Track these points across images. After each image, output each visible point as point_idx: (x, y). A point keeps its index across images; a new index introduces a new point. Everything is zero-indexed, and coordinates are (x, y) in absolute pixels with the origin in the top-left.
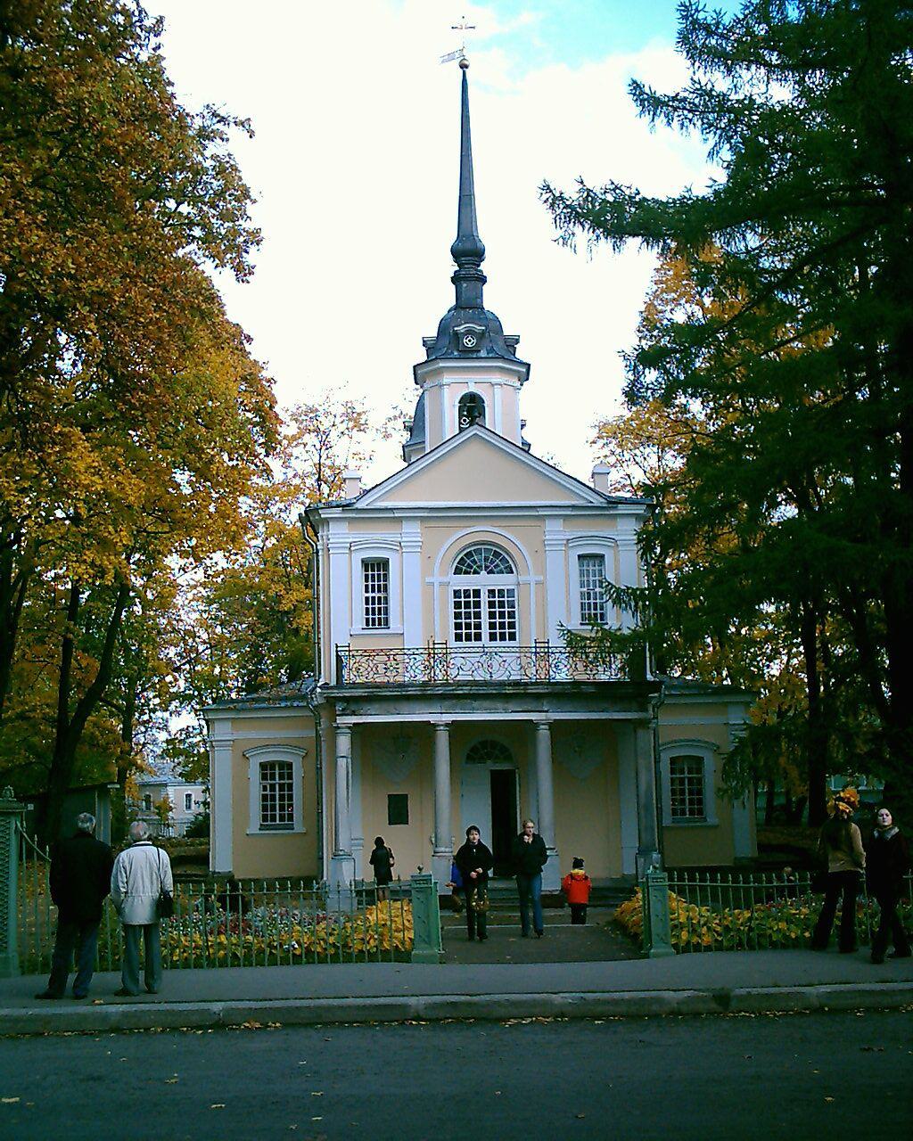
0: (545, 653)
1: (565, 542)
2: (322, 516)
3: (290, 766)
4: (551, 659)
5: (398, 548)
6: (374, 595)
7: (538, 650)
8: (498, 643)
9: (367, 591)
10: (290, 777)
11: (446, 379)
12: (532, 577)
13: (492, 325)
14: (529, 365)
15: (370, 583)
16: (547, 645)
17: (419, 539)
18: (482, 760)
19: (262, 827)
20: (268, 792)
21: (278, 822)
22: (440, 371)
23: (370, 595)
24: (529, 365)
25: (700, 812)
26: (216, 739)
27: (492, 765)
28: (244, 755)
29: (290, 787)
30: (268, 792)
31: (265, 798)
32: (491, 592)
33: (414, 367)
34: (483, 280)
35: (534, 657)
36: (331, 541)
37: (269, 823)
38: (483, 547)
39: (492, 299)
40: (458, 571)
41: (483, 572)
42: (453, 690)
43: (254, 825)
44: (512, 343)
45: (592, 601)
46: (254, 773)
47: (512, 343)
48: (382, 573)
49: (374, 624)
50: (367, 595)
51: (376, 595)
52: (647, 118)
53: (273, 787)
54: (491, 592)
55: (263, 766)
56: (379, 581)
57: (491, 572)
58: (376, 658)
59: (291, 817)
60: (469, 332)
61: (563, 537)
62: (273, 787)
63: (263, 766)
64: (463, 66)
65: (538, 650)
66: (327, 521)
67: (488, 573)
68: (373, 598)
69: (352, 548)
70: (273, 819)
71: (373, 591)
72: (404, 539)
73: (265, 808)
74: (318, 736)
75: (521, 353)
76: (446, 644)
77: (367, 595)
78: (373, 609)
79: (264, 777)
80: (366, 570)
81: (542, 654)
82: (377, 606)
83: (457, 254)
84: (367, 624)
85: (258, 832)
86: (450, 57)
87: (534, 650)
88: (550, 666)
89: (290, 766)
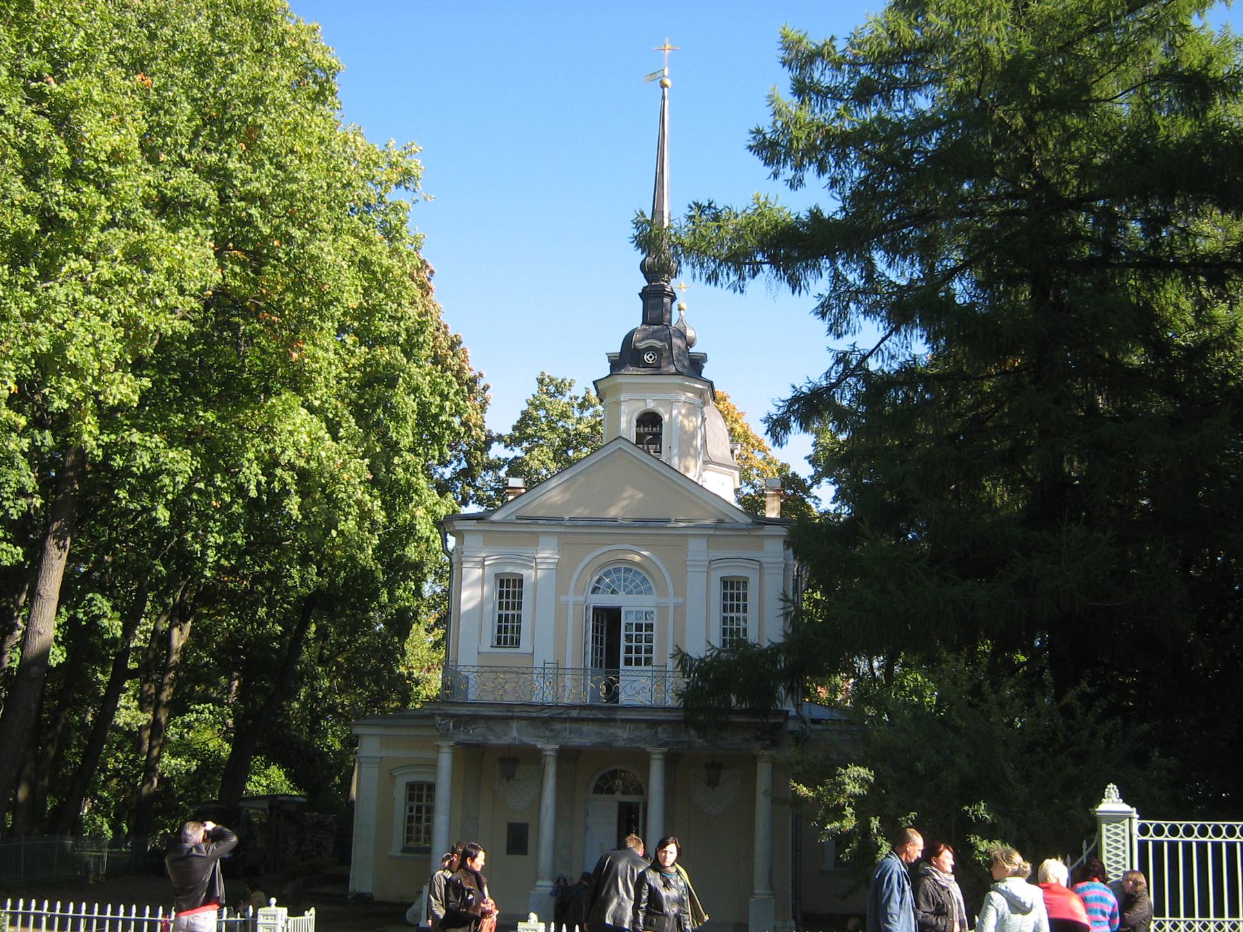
8: (633, 667)
9: (501, 608)
12: (671, 600)
16: (664, 669)
18: (611, 791)
19: (405, 850)
23: (504, 612)
26: (365, 755)
27: (619, 797)
30: (414, 813)
31: (410, 819)
35: (649, 682)
40: (595, 590)
43: (396, 850)
46: (400, 793)
48: (517, 590)
49: (505, 643)
51: (510, 612)
53: (419, 809)
56: (514, 598)
57: (630, 593)
58: (485, 675)
71: (507, 608)
73: (409, 830)
79: (411, 798)
80: (501, 586)
84: (499, 643)
85: (399, 854)
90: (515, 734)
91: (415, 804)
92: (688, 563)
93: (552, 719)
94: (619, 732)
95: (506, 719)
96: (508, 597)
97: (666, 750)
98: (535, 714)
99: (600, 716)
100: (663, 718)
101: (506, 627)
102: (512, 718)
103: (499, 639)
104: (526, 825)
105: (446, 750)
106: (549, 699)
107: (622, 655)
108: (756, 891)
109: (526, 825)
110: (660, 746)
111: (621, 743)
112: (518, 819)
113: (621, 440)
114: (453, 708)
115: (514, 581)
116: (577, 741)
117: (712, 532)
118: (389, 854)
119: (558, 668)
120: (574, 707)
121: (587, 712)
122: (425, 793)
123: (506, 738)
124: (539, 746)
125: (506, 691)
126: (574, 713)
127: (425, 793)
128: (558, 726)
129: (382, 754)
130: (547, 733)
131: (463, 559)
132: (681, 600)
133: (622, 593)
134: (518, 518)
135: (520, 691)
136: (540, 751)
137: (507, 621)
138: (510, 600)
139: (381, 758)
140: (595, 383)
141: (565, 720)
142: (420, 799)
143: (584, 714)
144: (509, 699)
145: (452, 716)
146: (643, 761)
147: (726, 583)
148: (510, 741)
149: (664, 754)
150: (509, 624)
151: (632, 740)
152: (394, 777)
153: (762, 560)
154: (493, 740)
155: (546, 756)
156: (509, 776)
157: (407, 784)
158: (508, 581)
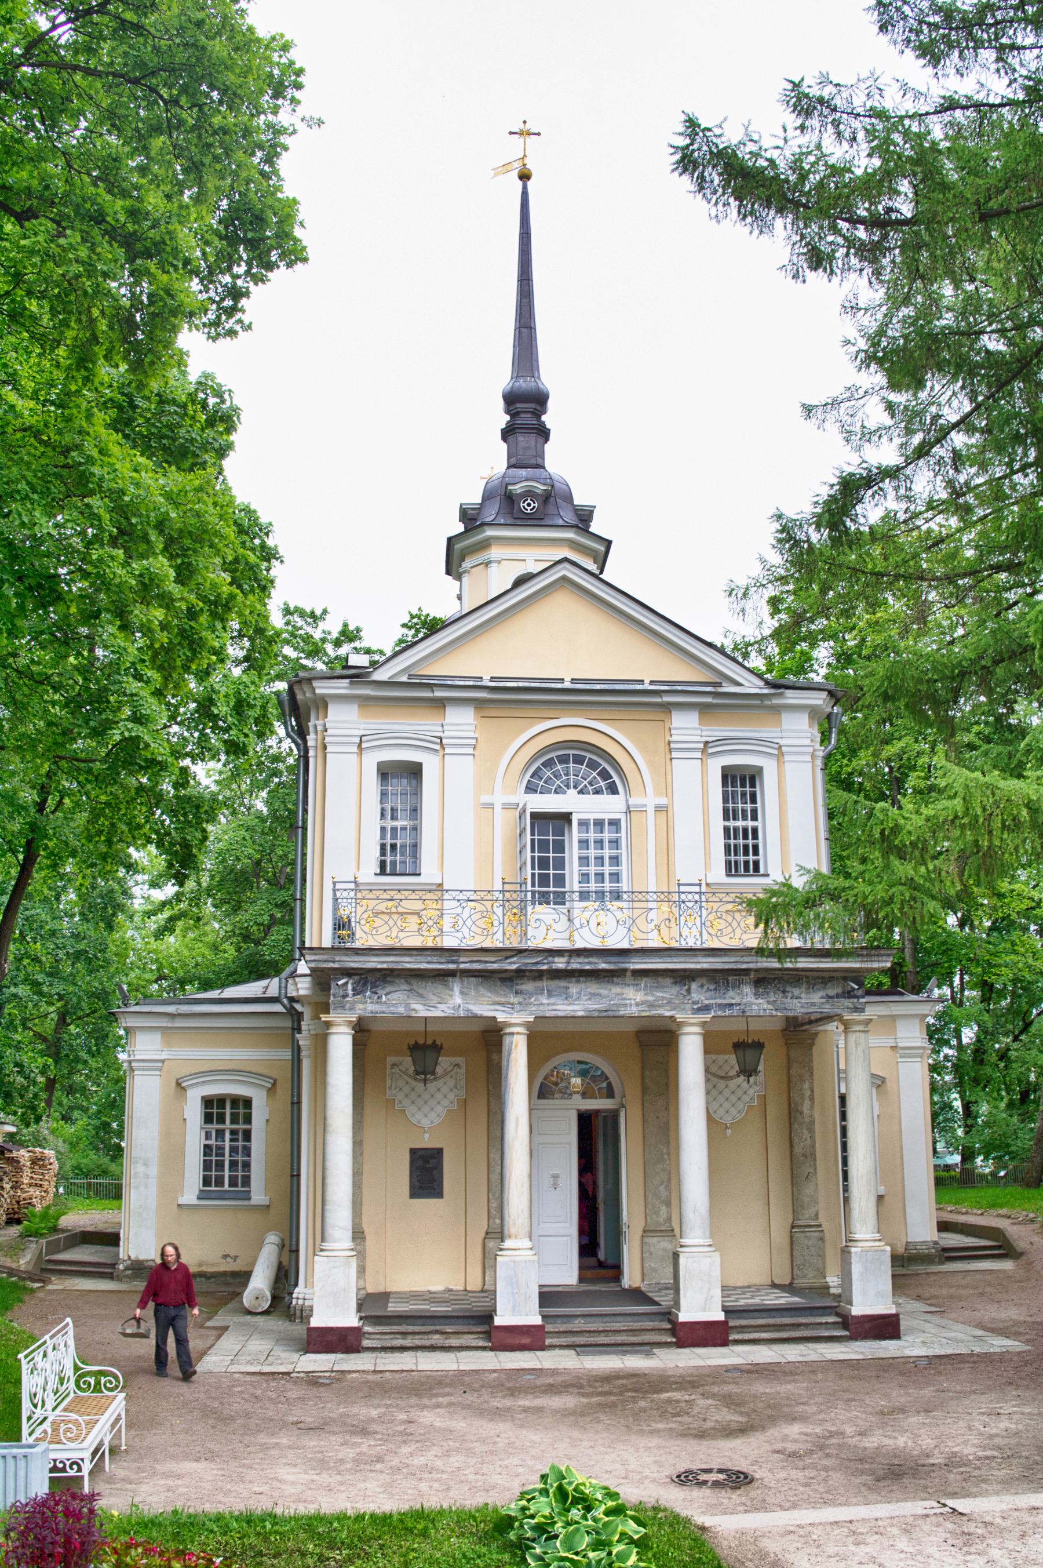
1: (701, 746)
2: (318, 691)
3: (248, 1102)
4: (704, 913)
5: (438, 747)
6: (395, 823)
7: (683, 897)
10: (248, 1120)
11: (495, 552)
12: (651, 800)
14: (609, 543)
17: (472, 734)
20: (212, 1142)
21: (226, 1187)
22: (485, 545)
24: (609, 543)
28: (178, 1084)
29: (247, 1135)
33: (449, 540)
34: (544, 434)
36: (330, 732)
37: (213, 1188)
38: (571, 752)
40: (530, 789)
41: (572, 792)
42: (537, 963)
43: (190, 1196)
46: (194, 1111)
53: (220, 1133)
54: (583, 824)
55: (208, 1102)
58: (403, 903)
59: (246, 1182)
60: (529, 494)
61: (698, 738)
62: (220, 1133)
63: (208, 1102)
64: (525, 177)
65: (683, 897)
66: (322, 704)
67: (581, 792)
69: (364, 745)
70: (220, 1182)
71: (394, 818)
72: (447, 734)
73: (207, 1165)
74: (297, 1050)
79: (208, 1118)
81: (690, 904)
85: (195, 1202)
86: (506, 167)
89: (248, 1102)
92: (673, 745)
93: (520, 974)
95: (442, 976)
97: (707, 1017)
98: (495, 966)
99: (603, 966)
100: (705, 966)
102: (452, 974)
103: (383, 864)
104: (440, 1151)
108: (857, 1236)
109: (440, 1151)
111: (633, 1011)
112: (426, 1142)
113: (566, 565)
114: (357, 958)
117: (708, 700)
118: (183, 1200)
120: (559, 953)
121: (581, 960)
122: (228, 1111)
123: (442, 1006)
124: (501, 1017)
126: (560, 963)
127: (228, 1111)
128: (528, 986)
129: (163, 1057)
131: (327, 740)
132: (663, 801)
133: (572, 792)
135: (465, 930)
139: (163, 1061)
141: (539, 975)
142: (221, 1119)
143: (576, 964)
144: (450, 942)
145: (349, 973)
148: (449, 1012)
149: (703, 1024)
151: (651, 1006)
152: (184, 1089)
153: (782, 742)
154: (421, 1010)
155: (513, 1034)
156: (425, 1072)
157: (203, 1098)
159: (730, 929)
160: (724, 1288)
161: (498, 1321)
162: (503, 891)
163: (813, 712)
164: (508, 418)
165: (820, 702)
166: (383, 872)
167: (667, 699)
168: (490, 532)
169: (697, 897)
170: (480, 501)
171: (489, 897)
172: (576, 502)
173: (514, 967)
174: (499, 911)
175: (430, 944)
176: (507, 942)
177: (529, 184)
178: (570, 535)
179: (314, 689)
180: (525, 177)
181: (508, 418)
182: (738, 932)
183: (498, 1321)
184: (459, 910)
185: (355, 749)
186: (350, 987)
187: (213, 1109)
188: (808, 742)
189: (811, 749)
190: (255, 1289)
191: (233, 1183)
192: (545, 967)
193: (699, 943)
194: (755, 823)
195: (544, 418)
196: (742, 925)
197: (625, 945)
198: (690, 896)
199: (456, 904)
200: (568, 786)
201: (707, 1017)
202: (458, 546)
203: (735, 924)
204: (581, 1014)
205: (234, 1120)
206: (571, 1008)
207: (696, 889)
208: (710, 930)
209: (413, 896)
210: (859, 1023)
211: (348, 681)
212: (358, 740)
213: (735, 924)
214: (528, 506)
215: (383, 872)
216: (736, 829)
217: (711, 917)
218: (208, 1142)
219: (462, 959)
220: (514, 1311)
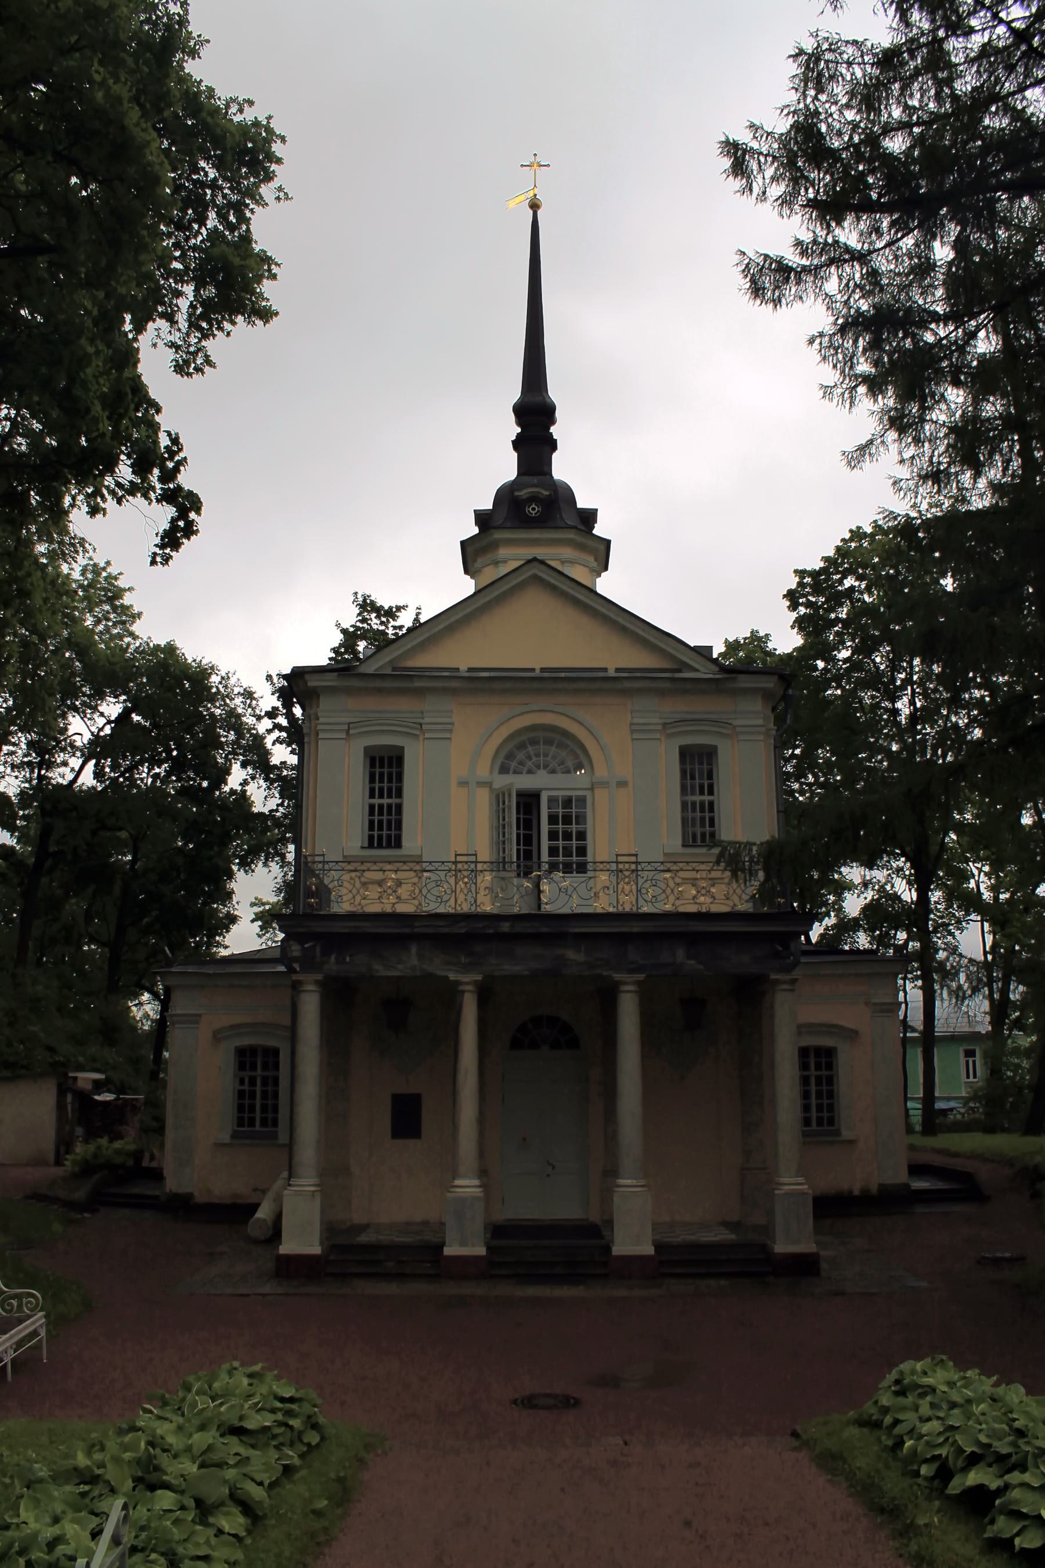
0: (633, 871)
1: (660, 727)
2: (310, 684)
3: (276, 1052)
4: (641, 881)
5: (417, 732)
6: (381, 801)
7: (621, 866)
9: (372, 795)
13: (563, 495)
15: (377, 785)
16: (633, 859)
19: (235, 1135)
20: (246, 1087)
21: (258, 1127)
22: (494, 546)
23: (376, 801)
24: (607, 543)
25: (831, 1121)
26: (179, 1012)
29: (276, 1081)
30: (246, 1087)
31: (241, 1094)
32: (552, 800)
34: (553, 445)
39: (561, 468)
41: (542, 773)
44: (589, 517)
45: (698, 814)
47: (589, 517)
48: (394, 770)
50: (372, 801)
51: (385, 801)
52: (752, 302)
53: (252, 1081)
54: (552, 800)
57: (553, 772)
58: (366, 874)
59: (275, 1123)
60: (533, 499)
64: (535, 206)
68: (381, 806)
69: (351, 732)
70: (252, 1122)
71: (381, 796)
72: (427, 720)
75: (599, 530)
76: (476, 855)
77: (372, 801)
78: (380, 822)
79: (241, 1066)
81: (627, 873)
82: (385, 818)
83: (521, 412)
87: (614, 866)
88: (639, 891)
89: (276, 1052)
90: (414, 961)
91: (247, 1074)
94: (571, 954)
96: (381, 781)
97: (641, 977)
98: (446, 930)
99: (545, 930)
101: (380, 822)
103: (371, 838)
105: (311, 987)
106: (465, 908)
107: (545, 857)
108: (782, 1180)
110: (631, 971)
115: (390, 759)
116: (510, 968)
119: (476, 862)
123: (400, 967)
124: (452, 976)
125: (398, 898)
126: (505, 927)
130: (463, 959)
134: (394, 669)
136: (458, 983)
137: (381, 813)
138: (385, 785)
140: (463, 543)
142: (254, 1067)
146: (608, 997)
147: (686, 754)
149: (639, 983)
150: (385, 818)
154: (380, 969)
155: (463, 992)
157: (236, 1048)
158: (382, 759)
159: (664, 896)
160: (653, 1224)
161: (447, 1251)
162: (455, 863)
163: (767, 695)
164: (519, 430)
165: (771, 685)
166: (371, 845)
167: (627, 685)
168: (498, 535)
169: (633, 867)
170: (491, 508)
171: (443, 868)
172: (579, 506)
173: (463, 931)
174: (452, 881)
175: (388, 909)
176: (459, 908)
177: (539, 212)
178: (571, 535)
179: (306, 683)
180: (535, 206)
181: (519, 430)
182: (672, 898)
183: (447, 1251)
184: (416, 880)
185: (344, 736)
186: (318, 949)
187: (245, 1057)
188: (760, 722)
189: (763, 729)
190: (258, 1219)
191: (264, 1122)
192: (491, 931)
193: (635, 909)
194: (711, 798)
195: (552, 429)
196: (676, 892)
197: (566, 910)
198: (627, 866)
199: (412, 874)
200: (538, 767)
201: (641, 977)
202: (469, 549)
203: (668, 891)
204: (527, 973)
205: (265, 1067)
206: (517, 968)
207: (633, 859)
208: (645, 897)
209: (375, 867)
210: (784, 982)
211: (336, 674)
212: (346, 727)
213: (668, 891)
214: (533, 510)
215: (371, 845)
216: (694, 804)
217: (647, 885)
218: (242, 1088)
219: (416, 924)
220: (463, 1243)
